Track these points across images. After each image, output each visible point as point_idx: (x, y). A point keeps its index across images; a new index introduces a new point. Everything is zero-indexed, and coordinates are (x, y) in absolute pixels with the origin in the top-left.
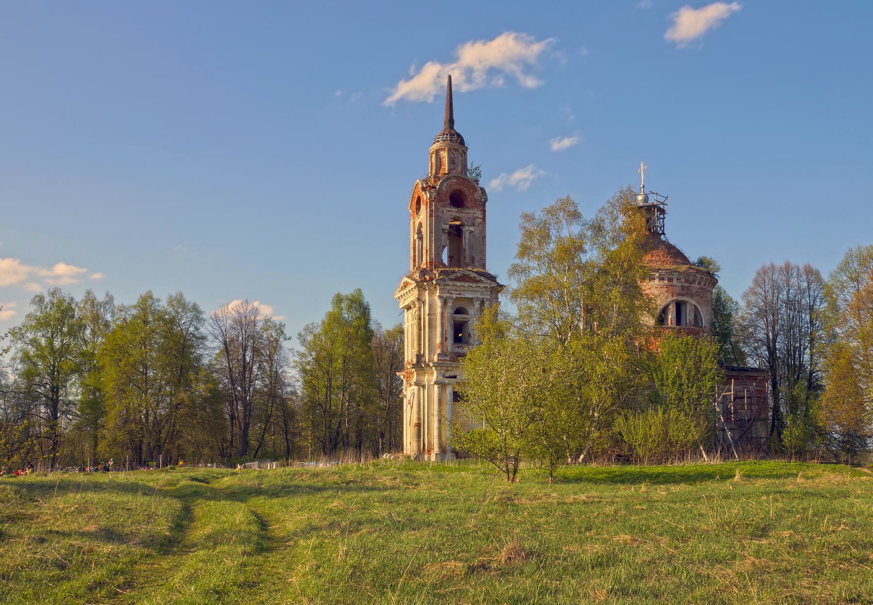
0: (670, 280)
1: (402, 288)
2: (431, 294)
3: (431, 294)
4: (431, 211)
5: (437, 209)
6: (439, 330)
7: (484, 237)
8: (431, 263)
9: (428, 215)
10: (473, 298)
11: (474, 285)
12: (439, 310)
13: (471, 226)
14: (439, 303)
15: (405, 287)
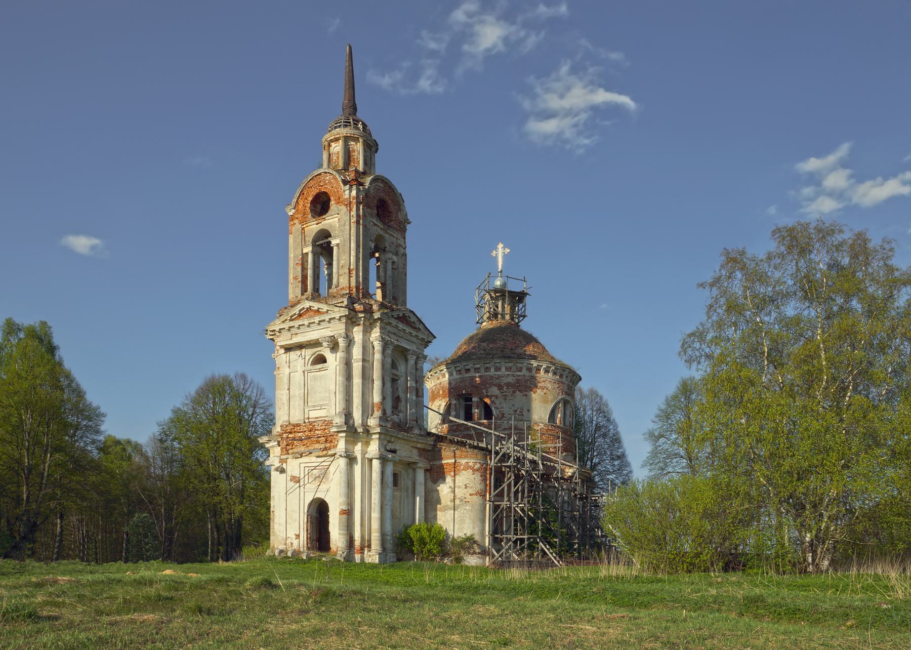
0: (561, 376)
1: (291, 317)
2: (367, 331)
3: (367, 331)
4: (358, 216)
5: (364, 215)
6: (377, 384)
7: (405, 274)
8: (357, 288)
9: (354, 219)
10: (407, 350)
11: (414, 333)
12: (378, 356)
13: (395, 255)
14: (378, 346)
15: (300, 315)
